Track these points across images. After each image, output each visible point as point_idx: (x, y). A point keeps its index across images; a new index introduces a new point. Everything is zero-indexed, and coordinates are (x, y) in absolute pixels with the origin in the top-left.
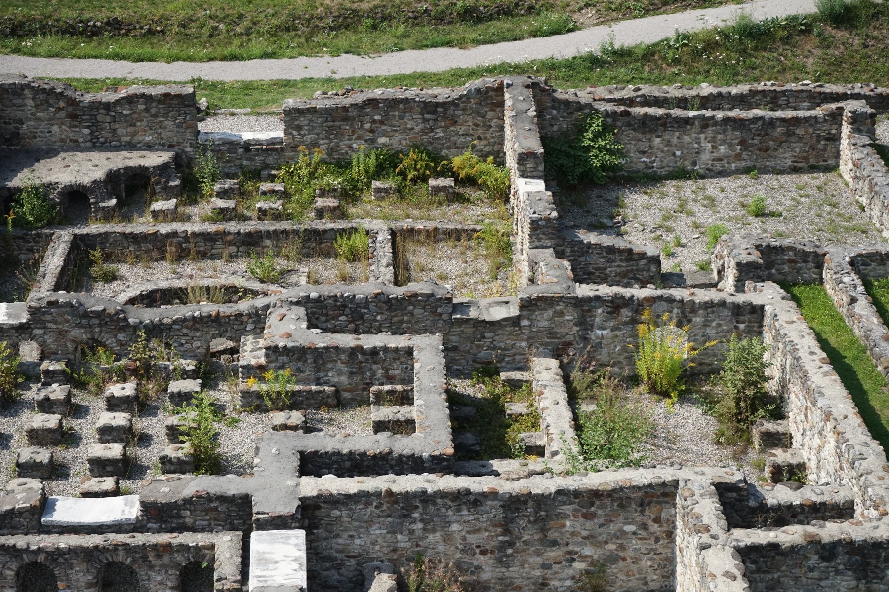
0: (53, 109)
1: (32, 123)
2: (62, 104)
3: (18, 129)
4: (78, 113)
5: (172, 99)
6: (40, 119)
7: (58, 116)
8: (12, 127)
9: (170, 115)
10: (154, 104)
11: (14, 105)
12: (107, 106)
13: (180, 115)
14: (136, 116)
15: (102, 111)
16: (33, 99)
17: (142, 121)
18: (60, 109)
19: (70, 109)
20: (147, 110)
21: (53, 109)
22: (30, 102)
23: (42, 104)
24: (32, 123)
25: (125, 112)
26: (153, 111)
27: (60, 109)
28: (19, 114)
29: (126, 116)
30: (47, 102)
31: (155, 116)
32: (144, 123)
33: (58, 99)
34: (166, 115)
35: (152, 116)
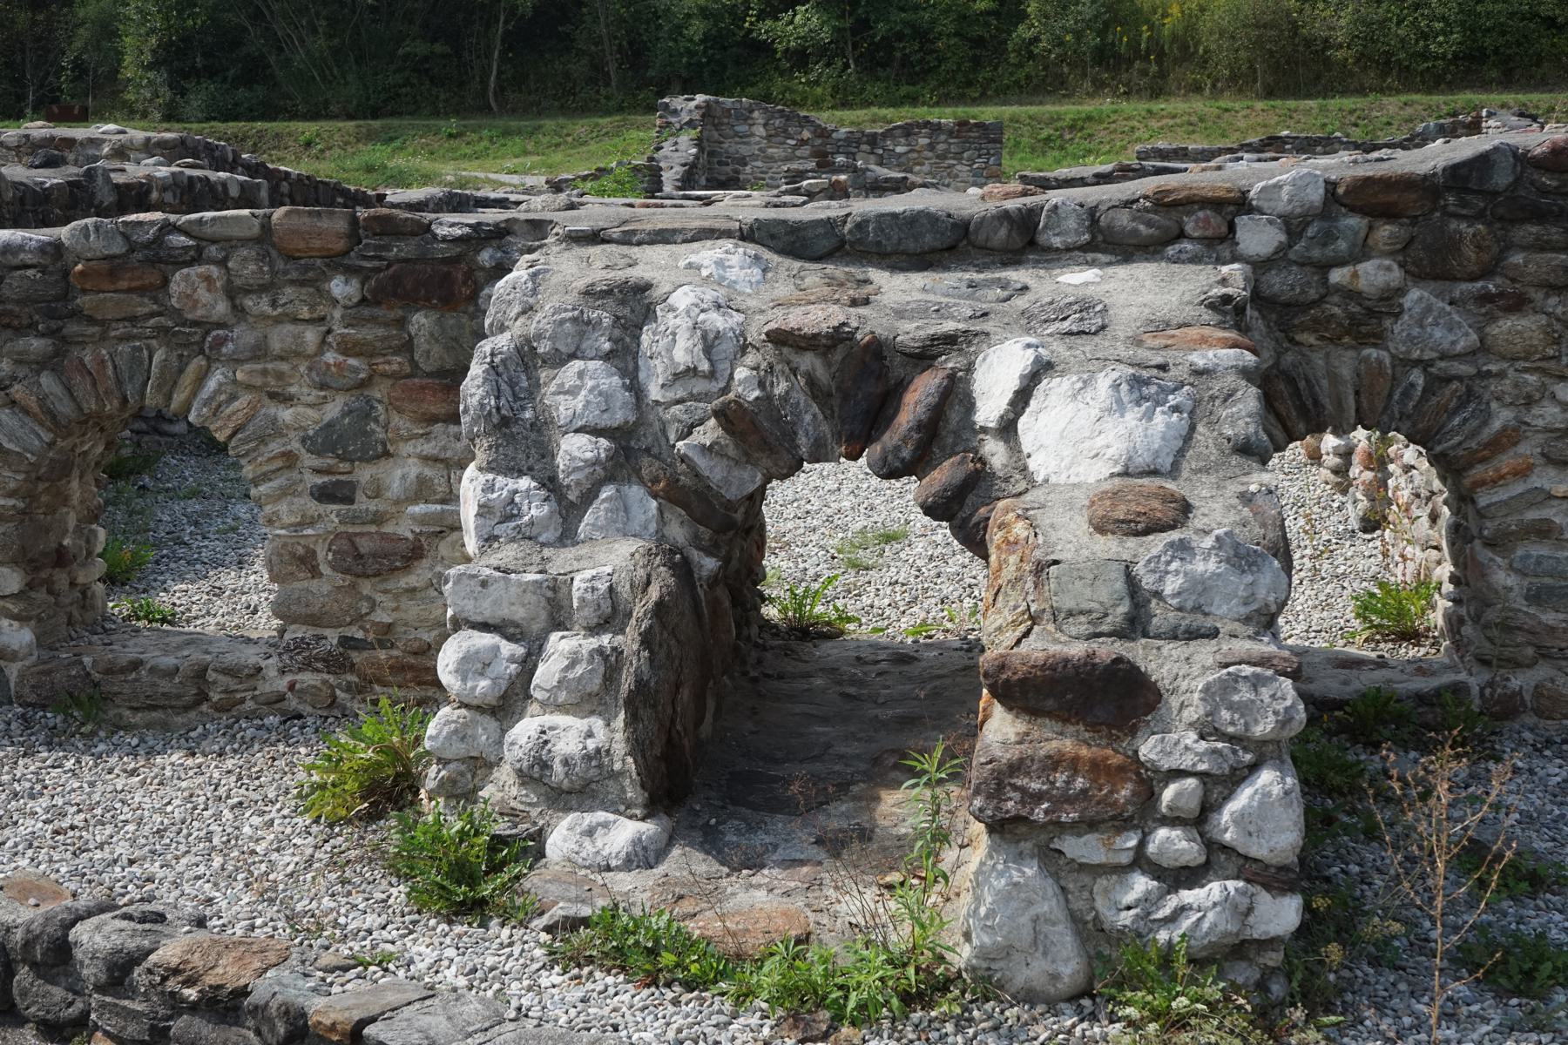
0: (793, 142)
1: (759, 164)
2: (806, 134)
3: (737, 172)
4: (829, 148)
5: (970, 130)
6: (771, 159)
7: (798, 153)
8: (728, 169)
9: (965, 155)
10: (943, 137)
11: (736, 134)
12: (873, 140)
13: (979, 156)
14: (915, 155)
15: (865, 147)
16: (765, 125)
17: (922, 164)
18: (803, 142)
19: (819, 142)
20: (931, 147)
21: (793, 142)
22: (760, 131)
23: (776, 135)
24: (759, 164)
25: (899, 149)
26: (941, 147)
27: (803, 142)
28: (744, 150)
29: (900, 155)
30: (785, 131)
31: (943, 157)
32: (926, 168)
33: (802, 127)
34: (958, 156)
35: (938, 157)
